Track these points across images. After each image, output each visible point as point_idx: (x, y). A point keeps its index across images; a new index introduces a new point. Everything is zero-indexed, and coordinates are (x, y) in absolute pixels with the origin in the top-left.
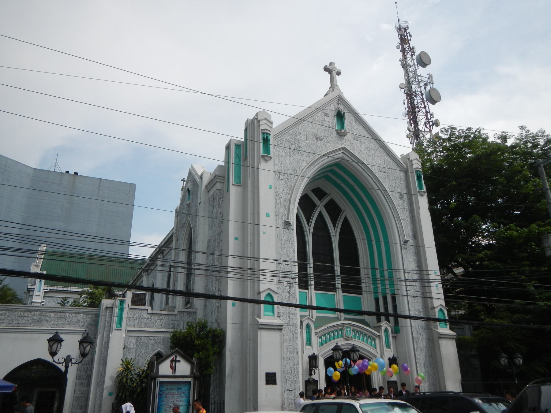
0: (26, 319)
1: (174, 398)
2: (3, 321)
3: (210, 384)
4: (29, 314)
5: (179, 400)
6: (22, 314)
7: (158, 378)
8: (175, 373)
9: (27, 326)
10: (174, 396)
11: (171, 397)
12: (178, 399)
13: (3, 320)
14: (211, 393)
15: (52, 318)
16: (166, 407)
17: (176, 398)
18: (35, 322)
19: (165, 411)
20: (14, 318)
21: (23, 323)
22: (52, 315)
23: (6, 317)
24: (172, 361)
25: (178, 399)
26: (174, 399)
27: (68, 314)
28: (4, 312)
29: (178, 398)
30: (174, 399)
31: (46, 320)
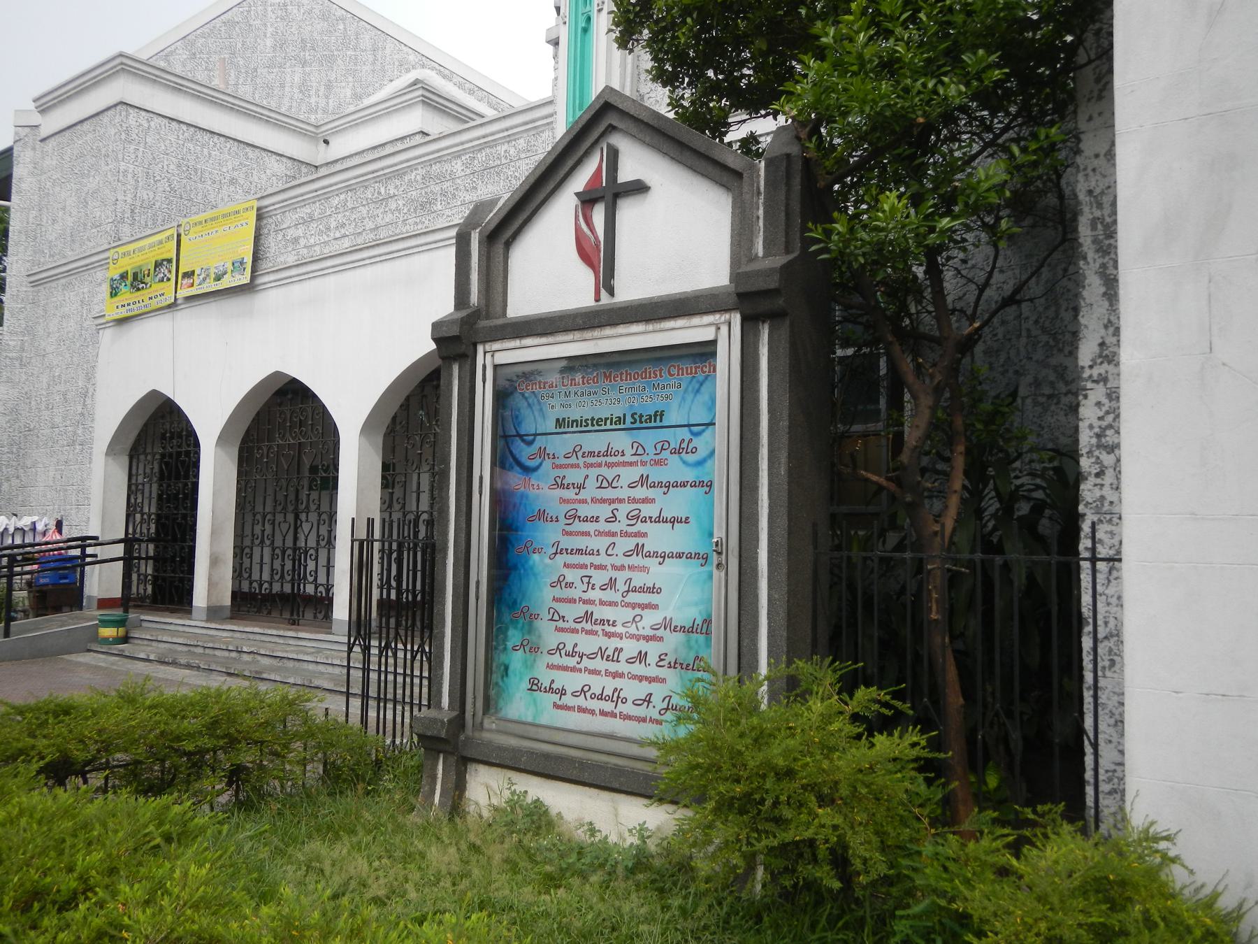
0: (393, 206)
1: (609, 494)
2: (343, 231)
3: (1079, 370)
4: (398, 182)
5: (648, 511)
6: (383, 190)
7: (484, 342)
8: (611, 292)
9: (398, 231)
10: (609, 473)
11: (590, 491)
12: (645, 501)
13: (343, 225)
14: (1085, 463)
15: (458, 181)
16: (566, 566)
17: (624, 493)
18: (415, 211)
19: (557, 592)
20: (364, 210)
21: (388, 224)
22: (458, 166)
23: (347, 214)
24: (587, 200)
25: (645, 501)
26: (611, 501)
27: (505, 147)
28: (342, 197)
29: (641, 492)
30: (611, 501)
31: (444, 194)
